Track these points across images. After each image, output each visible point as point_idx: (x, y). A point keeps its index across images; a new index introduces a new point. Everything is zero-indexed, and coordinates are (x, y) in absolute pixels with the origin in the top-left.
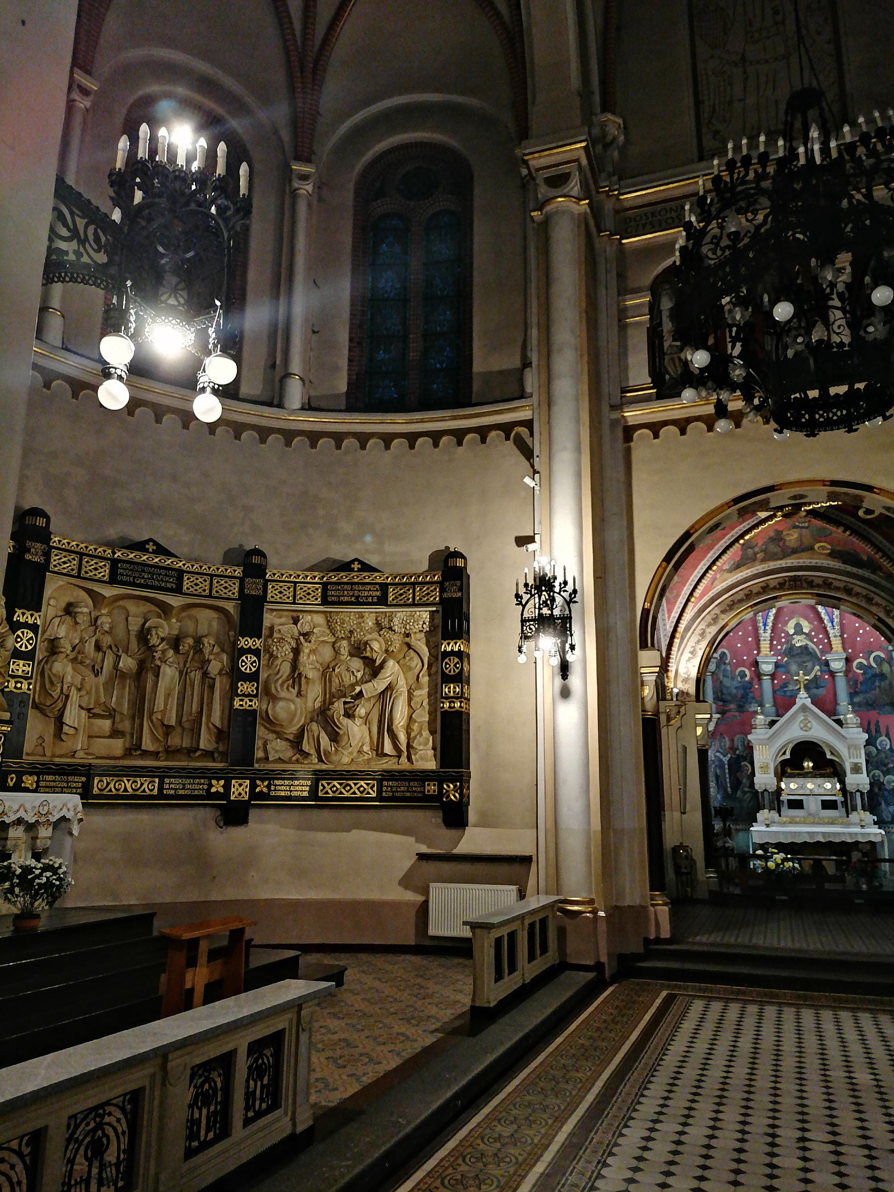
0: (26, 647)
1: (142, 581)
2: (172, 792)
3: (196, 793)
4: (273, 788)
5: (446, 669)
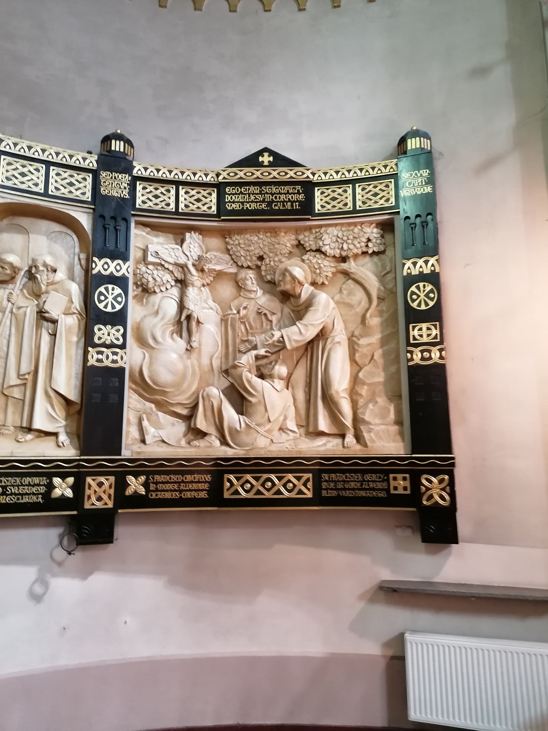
3: (26, 500)
4: (152, 487)
5: (413, 301)
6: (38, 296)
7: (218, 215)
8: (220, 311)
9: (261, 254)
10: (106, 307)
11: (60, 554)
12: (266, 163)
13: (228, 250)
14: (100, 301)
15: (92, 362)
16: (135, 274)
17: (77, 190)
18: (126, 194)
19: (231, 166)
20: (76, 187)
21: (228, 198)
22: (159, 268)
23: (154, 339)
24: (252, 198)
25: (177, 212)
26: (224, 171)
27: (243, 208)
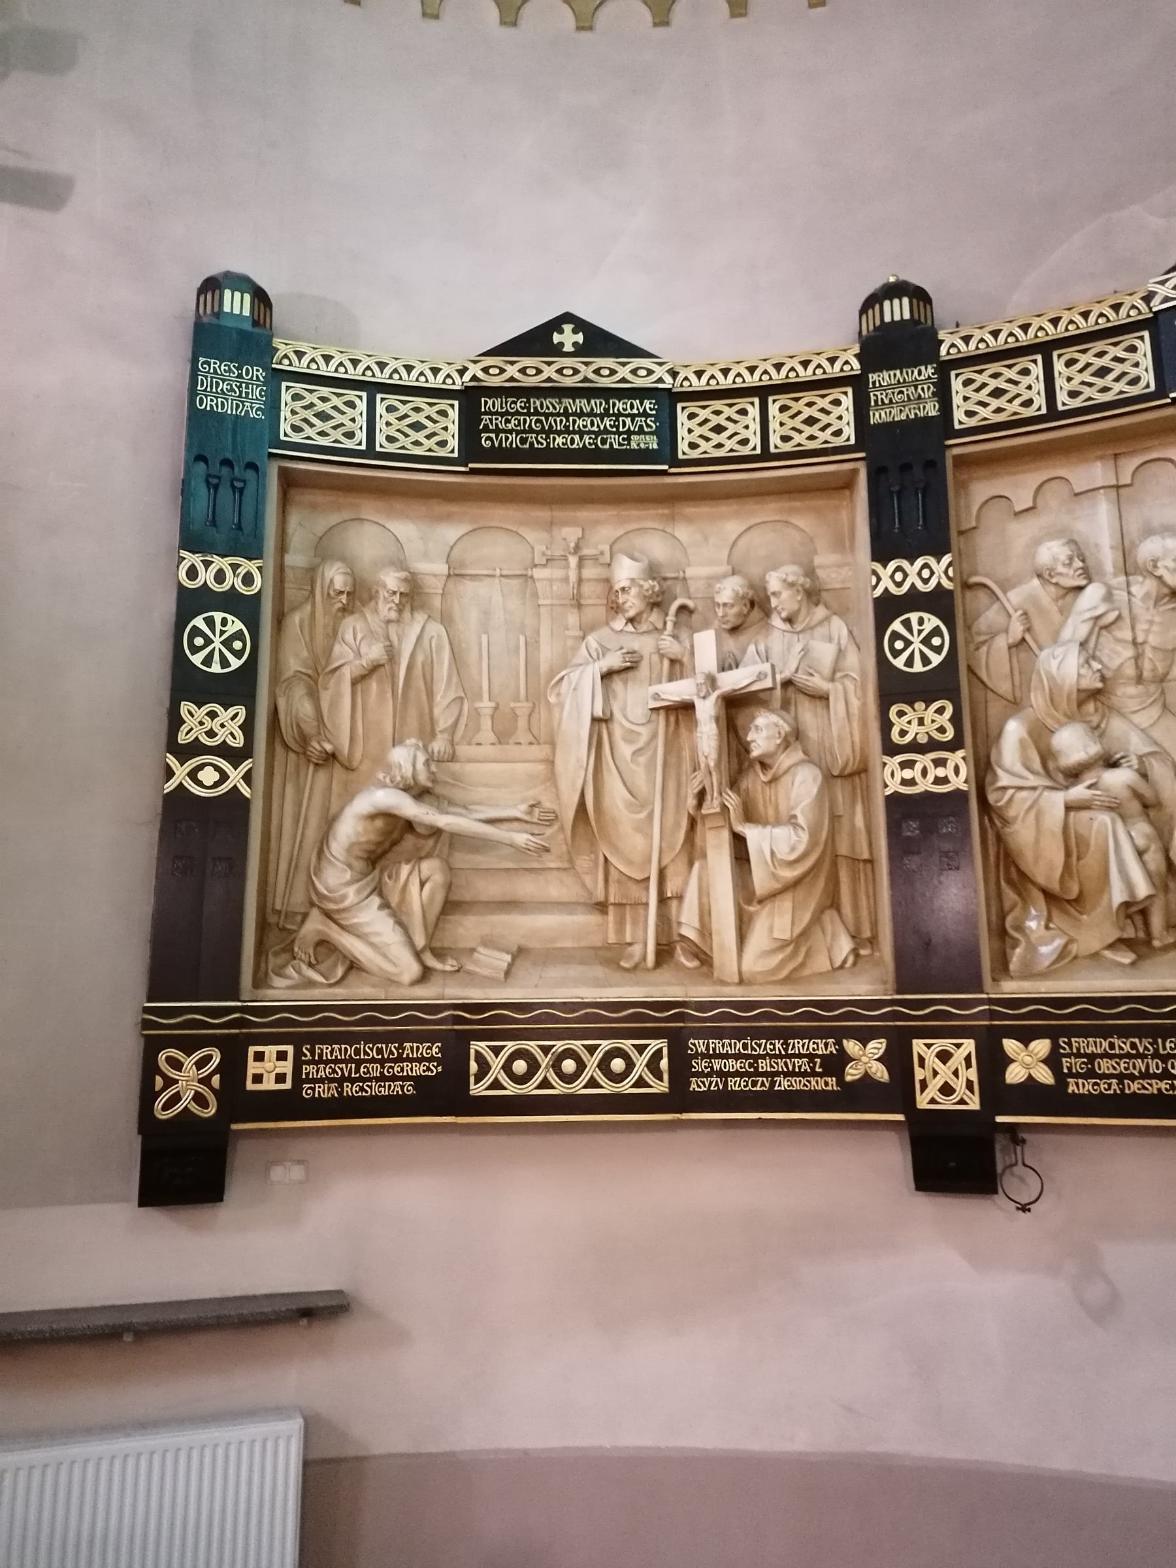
10: (910, 662)
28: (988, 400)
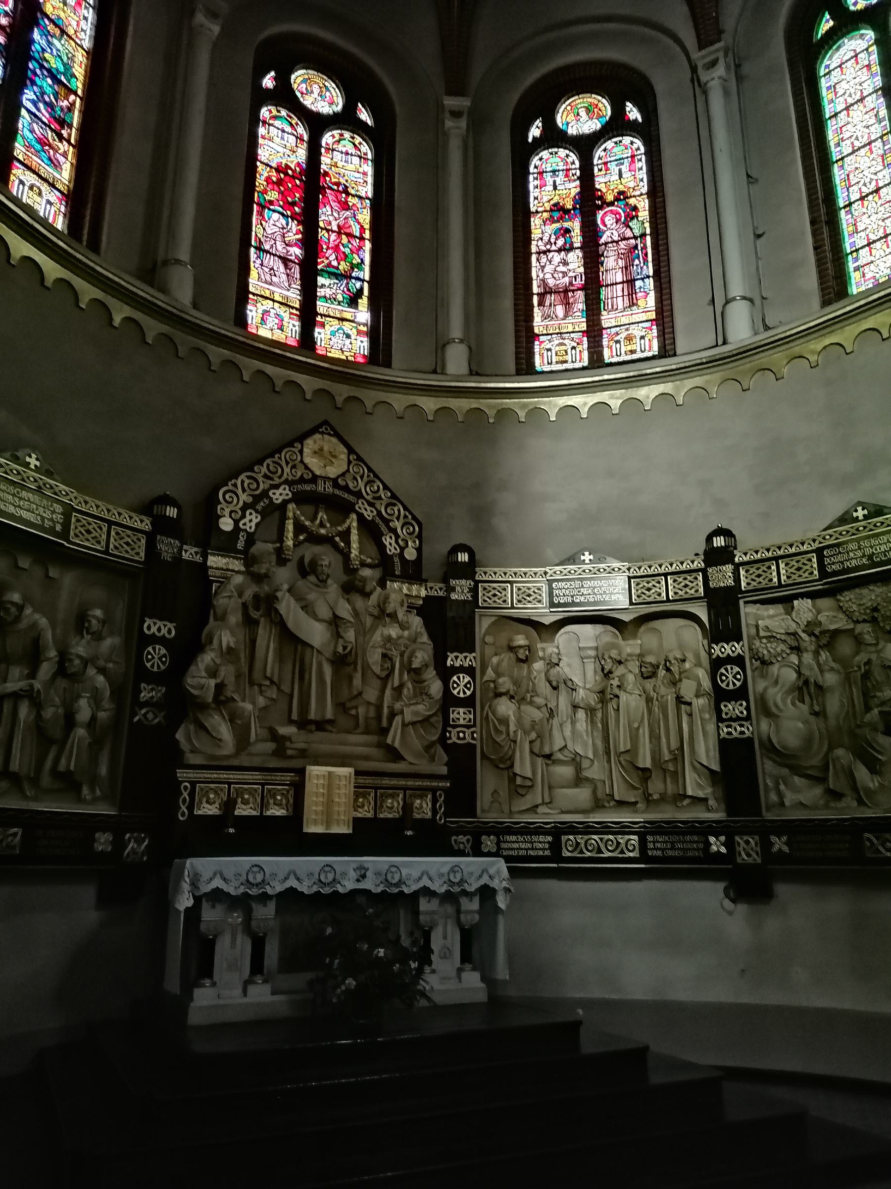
0: (464, 693)
1: (582, 599)
2: (659, 853)
3: (690, 854)
6: (674, 683)
7: (820, 580)
8: (842, 670)
9: (875, 605)
10: (728, 685)
11: (727, 903)
12: (861, 518)
13: (841, 608)
14: (722, 681)
15: (723, 735)
16: (750, 649)
17: (690, 589)
18: (731, 582)
19: (825, 530)
20: (690, 587)
21: (827, 561)
22: (772, 640)
23: (776, 705)
24: (851, 554)
25: (780, 585)
26: (819, 536)
27: (844, 567)
28: (762, 573)
